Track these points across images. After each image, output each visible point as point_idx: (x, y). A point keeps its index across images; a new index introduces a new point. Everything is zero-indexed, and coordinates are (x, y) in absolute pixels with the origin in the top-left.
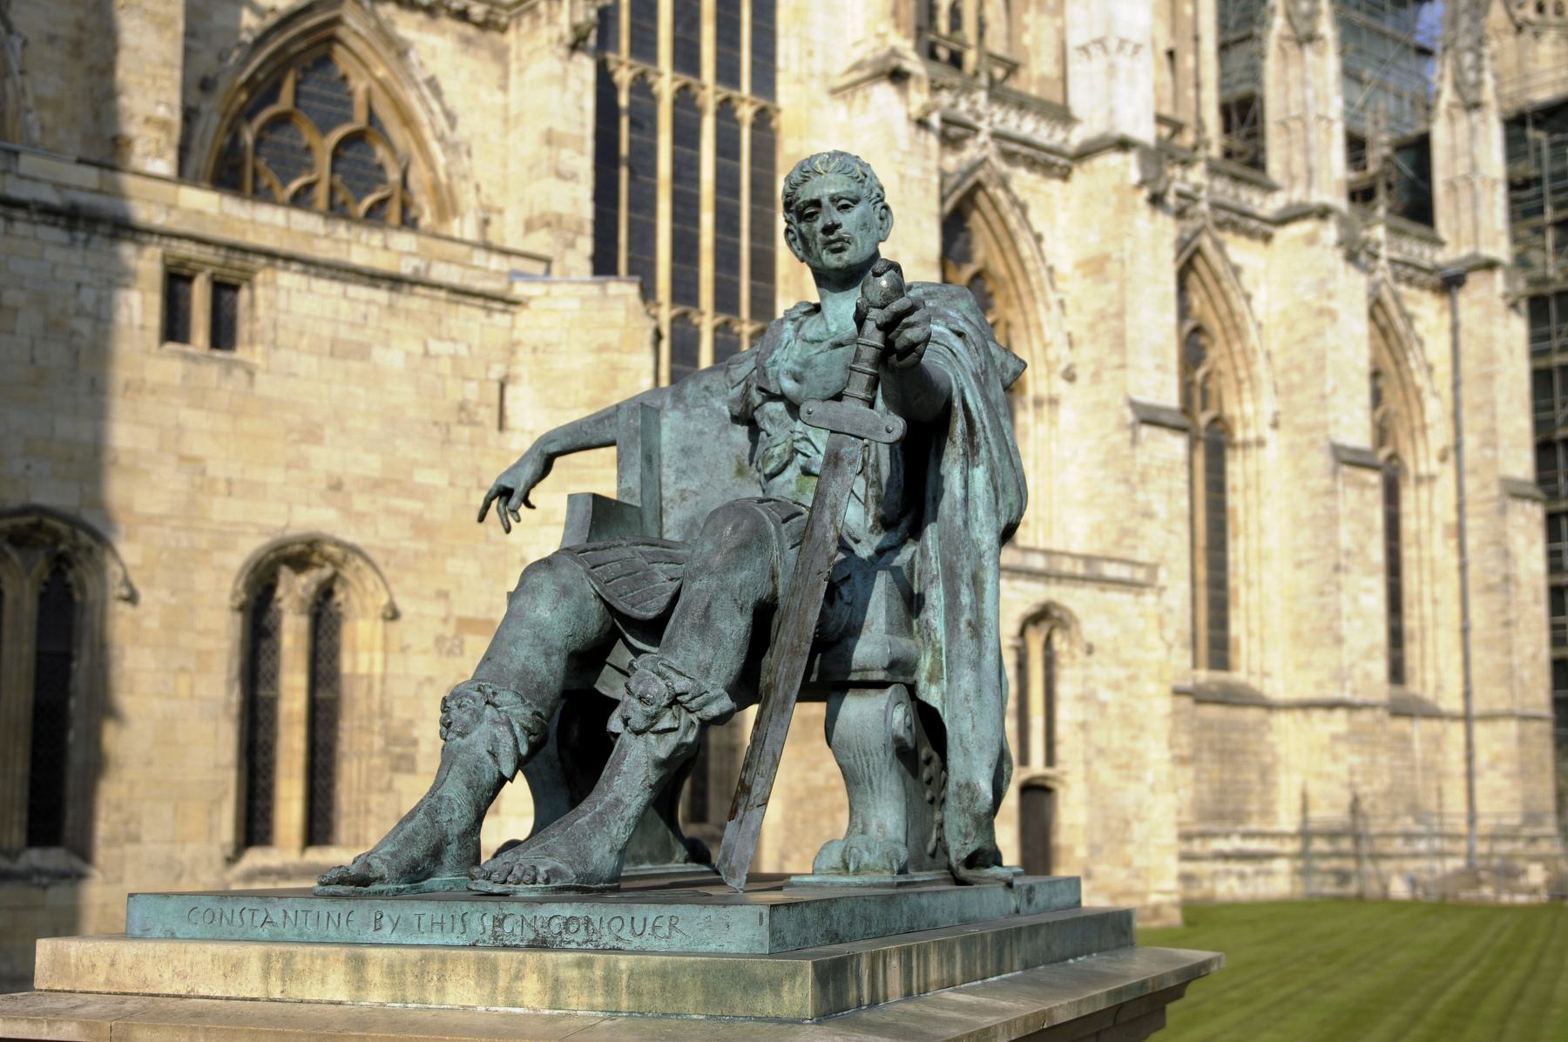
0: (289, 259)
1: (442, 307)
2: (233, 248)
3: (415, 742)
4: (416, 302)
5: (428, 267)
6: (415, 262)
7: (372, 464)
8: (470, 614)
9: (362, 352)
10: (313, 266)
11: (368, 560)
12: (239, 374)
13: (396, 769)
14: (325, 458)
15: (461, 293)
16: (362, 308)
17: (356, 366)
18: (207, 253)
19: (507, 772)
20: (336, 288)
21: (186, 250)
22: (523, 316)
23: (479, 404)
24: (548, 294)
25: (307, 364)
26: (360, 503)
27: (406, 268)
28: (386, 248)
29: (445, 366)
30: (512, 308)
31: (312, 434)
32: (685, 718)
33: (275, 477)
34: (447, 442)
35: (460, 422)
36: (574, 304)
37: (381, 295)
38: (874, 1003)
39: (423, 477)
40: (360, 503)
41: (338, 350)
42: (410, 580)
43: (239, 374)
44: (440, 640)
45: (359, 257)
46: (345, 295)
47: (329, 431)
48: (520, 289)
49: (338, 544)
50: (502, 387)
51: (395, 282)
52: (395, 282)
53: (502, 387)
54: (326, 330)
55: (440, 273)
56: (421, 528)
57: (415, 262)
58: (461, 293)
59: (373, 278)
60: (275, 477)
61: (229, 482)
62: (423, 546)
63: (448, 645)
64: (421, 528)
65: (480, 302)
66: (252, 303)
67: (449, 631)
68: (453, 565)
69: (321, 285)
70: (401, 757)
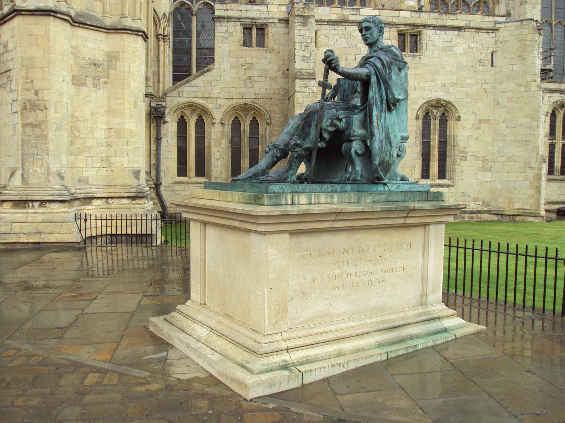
0: (429, 26)
1: (474, 34)
2: (414, 25)
3: (467, 153)
4: (467, 33)
5: (470, 23)
6: (466, 22)
7: (454, 79)
8: (483, 118)
9: (451, 49)
10: (435, 27)
11: (453, 105)
12: (417, 58)
13: (461, 160)
14: (440, 79)
15: (479, 29)
16: (450, 37)
17: (449, 53)
18: (408, 28)
19: (275, 159)
20: (443, 32)
21: (402, 27)
22: (499, 34)
23: (485, 60)
24: (505, 26)
25: (435, 54)
26: (451, 90)
27: (462, 24)
28: (457, 19)
29: (475, 50)
30: (495, 32)
31: (437, 72)
32: (300, 148)
33: (427, 84)
34: (475, 71)
35: (480, 65)
36: (513, 28)
37: (456, 33)
38: (292, 204)
39: (469, 81)
40: (451, 90)
41: (444, 49)
42: (465, 110)
43: (417, 58)
44: (473, 125)
45: (449, 23)
46: (445, 34)
47: (441, 71)
48: (497, 26)
49: (444, 101)
50: (492, 54)
51: (459, 29)
52: (459, 29)
53: (492, 54)
54: (440, 44)
55: (473, 25)
56: (467, 95)
57: (466, 22)
58: (479, 29)
59: (454, 28)
60: (427, 84)
61: (415, 86)
62: (469, 100)
63: (476, 126)
64: (467, 95)
65: (485, 31)
66: (420, 40)
67: (476, 123)
68: (477, 105)
69: (438, 32)
70: (463, 156)
